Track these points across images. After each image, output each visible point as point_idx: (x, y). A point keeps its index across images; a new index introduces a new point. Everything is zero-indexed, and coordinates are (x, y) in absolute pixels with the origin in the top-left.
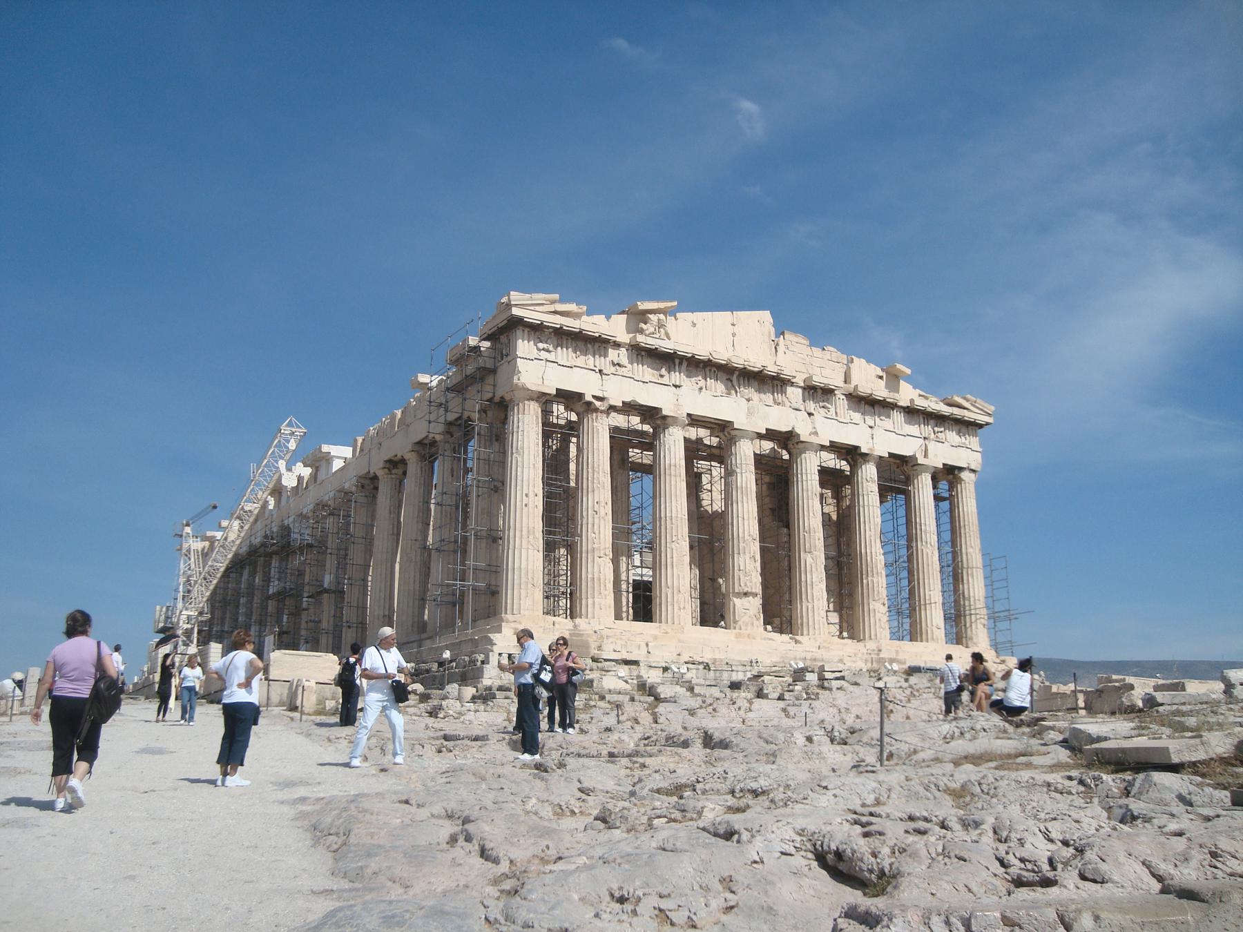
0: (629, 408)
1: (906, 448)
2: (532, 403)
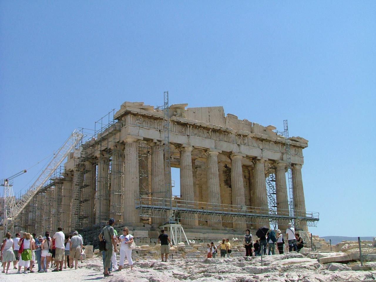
1: (276, 156)
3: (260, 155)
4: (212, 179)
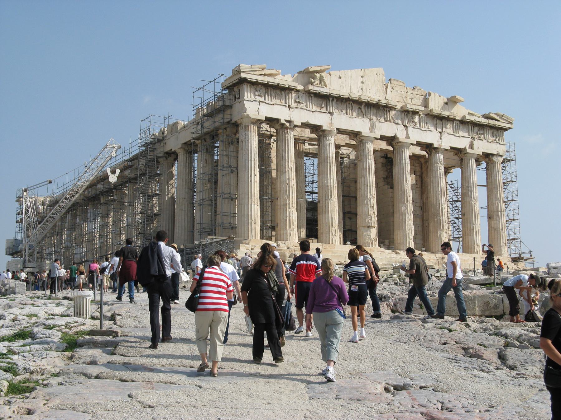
0: (305, 125)
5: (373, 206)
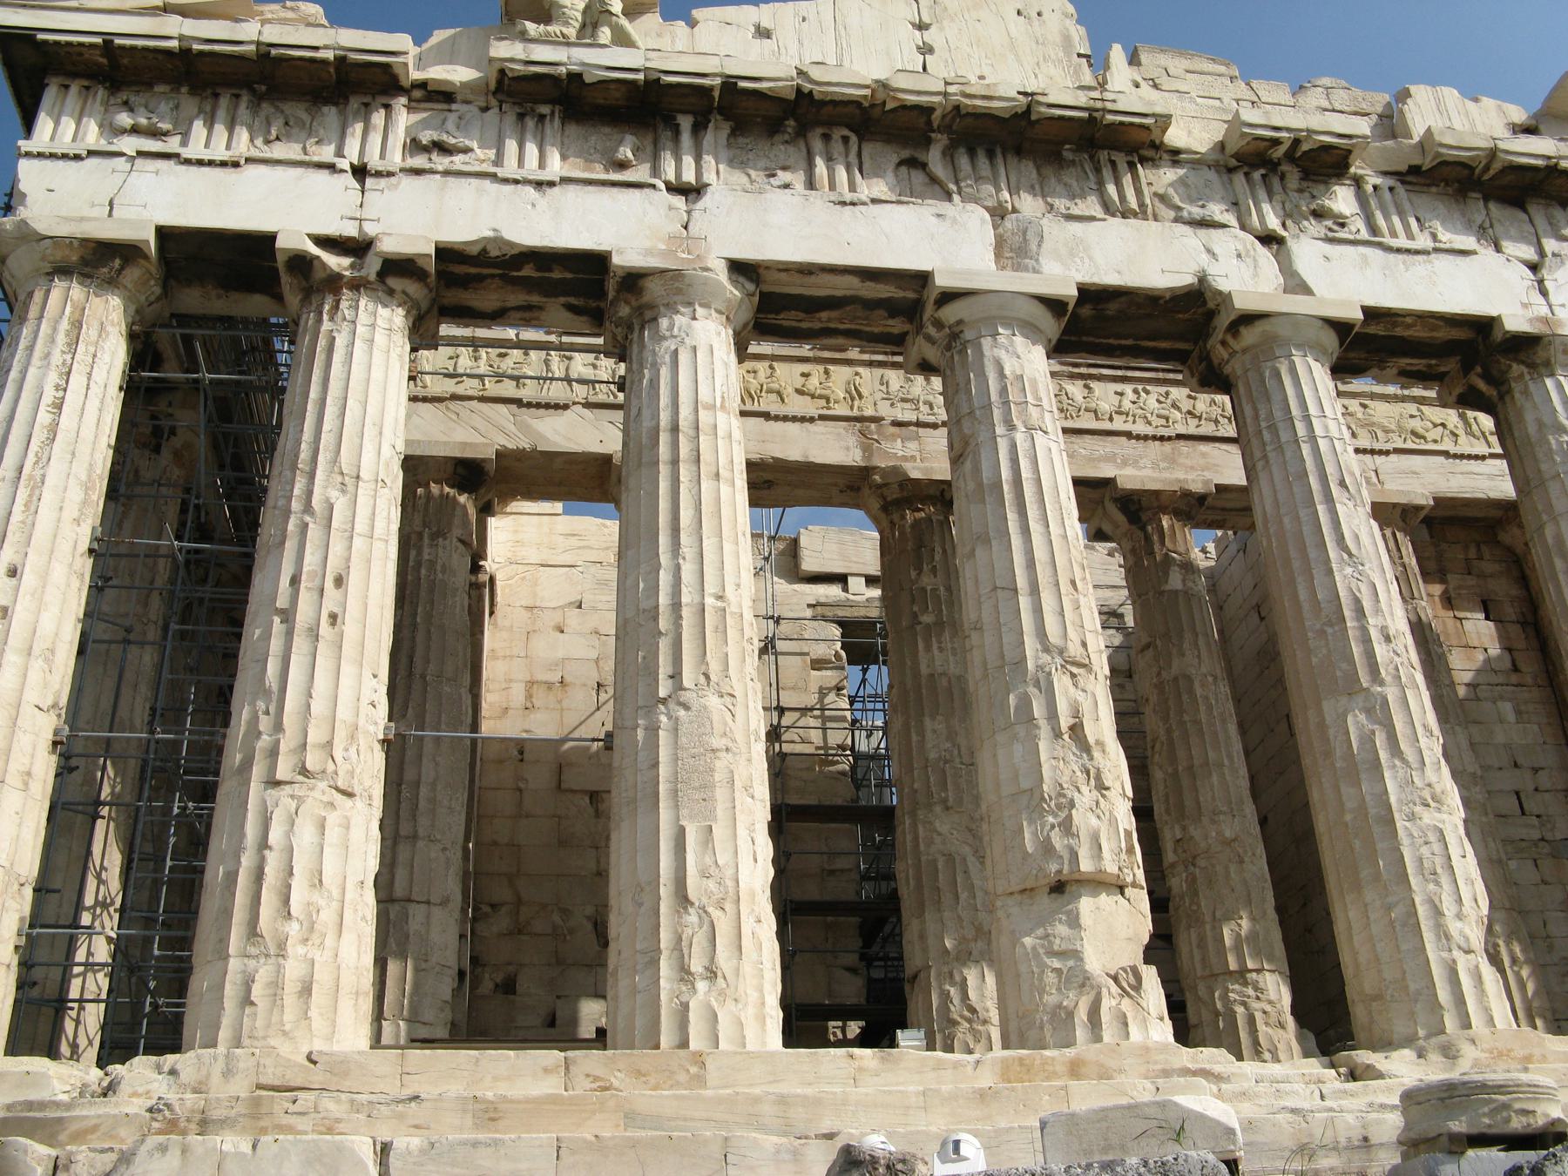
2: (59, 285)
3: (1525, 306)
4: (988, 541)
5: (1077, 730)
